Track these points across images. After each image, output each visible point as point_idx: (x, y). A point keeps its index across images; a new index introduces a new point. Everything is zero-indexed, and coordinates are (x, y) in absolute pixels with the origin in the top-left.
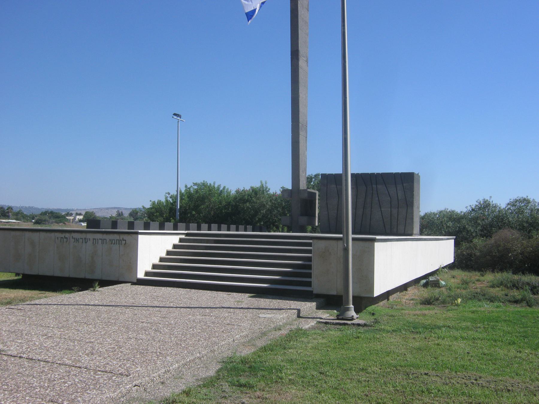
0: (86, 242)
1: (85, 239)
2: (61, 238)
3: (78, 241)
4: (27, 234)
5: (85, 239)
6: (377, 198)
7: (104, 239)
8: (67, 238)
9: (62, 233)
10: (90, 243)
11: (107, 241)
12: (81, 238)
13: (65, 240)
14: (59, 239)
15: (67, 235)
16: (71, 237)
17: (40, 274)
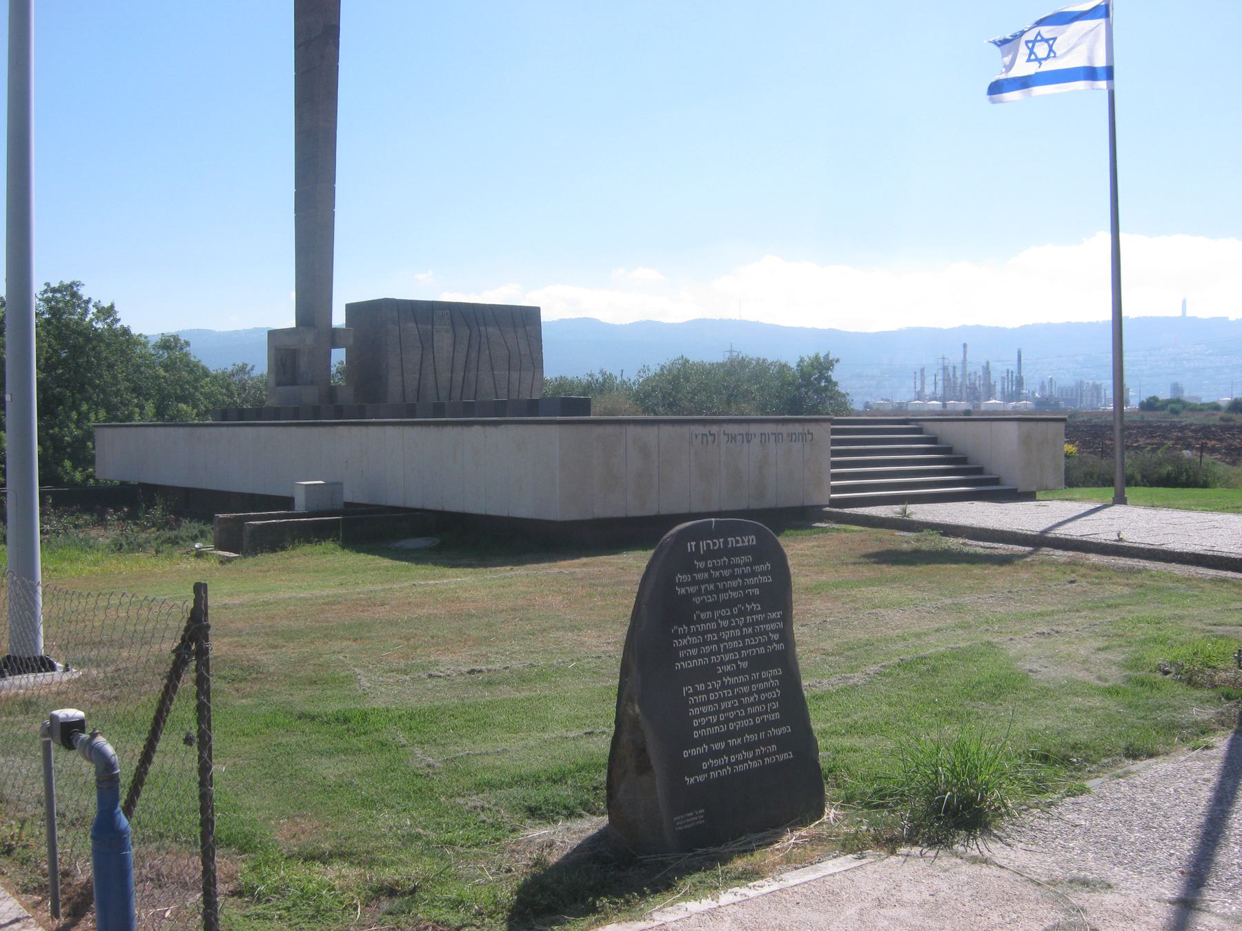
0: (748, 441)
1: (747, 434)
2: (703, 435)
3: (734, 439)
4: (631, 430)
5: (747, 434)
6: (488, 352)
7: (779, 434)
8: (714, 435)
10: (756, 441)
11: (785, 435)
12: (740, 434)
13: (711, 438)
14: (700, 437)
15: (714, 429)
16: (722, 432)
17: (663, 512)
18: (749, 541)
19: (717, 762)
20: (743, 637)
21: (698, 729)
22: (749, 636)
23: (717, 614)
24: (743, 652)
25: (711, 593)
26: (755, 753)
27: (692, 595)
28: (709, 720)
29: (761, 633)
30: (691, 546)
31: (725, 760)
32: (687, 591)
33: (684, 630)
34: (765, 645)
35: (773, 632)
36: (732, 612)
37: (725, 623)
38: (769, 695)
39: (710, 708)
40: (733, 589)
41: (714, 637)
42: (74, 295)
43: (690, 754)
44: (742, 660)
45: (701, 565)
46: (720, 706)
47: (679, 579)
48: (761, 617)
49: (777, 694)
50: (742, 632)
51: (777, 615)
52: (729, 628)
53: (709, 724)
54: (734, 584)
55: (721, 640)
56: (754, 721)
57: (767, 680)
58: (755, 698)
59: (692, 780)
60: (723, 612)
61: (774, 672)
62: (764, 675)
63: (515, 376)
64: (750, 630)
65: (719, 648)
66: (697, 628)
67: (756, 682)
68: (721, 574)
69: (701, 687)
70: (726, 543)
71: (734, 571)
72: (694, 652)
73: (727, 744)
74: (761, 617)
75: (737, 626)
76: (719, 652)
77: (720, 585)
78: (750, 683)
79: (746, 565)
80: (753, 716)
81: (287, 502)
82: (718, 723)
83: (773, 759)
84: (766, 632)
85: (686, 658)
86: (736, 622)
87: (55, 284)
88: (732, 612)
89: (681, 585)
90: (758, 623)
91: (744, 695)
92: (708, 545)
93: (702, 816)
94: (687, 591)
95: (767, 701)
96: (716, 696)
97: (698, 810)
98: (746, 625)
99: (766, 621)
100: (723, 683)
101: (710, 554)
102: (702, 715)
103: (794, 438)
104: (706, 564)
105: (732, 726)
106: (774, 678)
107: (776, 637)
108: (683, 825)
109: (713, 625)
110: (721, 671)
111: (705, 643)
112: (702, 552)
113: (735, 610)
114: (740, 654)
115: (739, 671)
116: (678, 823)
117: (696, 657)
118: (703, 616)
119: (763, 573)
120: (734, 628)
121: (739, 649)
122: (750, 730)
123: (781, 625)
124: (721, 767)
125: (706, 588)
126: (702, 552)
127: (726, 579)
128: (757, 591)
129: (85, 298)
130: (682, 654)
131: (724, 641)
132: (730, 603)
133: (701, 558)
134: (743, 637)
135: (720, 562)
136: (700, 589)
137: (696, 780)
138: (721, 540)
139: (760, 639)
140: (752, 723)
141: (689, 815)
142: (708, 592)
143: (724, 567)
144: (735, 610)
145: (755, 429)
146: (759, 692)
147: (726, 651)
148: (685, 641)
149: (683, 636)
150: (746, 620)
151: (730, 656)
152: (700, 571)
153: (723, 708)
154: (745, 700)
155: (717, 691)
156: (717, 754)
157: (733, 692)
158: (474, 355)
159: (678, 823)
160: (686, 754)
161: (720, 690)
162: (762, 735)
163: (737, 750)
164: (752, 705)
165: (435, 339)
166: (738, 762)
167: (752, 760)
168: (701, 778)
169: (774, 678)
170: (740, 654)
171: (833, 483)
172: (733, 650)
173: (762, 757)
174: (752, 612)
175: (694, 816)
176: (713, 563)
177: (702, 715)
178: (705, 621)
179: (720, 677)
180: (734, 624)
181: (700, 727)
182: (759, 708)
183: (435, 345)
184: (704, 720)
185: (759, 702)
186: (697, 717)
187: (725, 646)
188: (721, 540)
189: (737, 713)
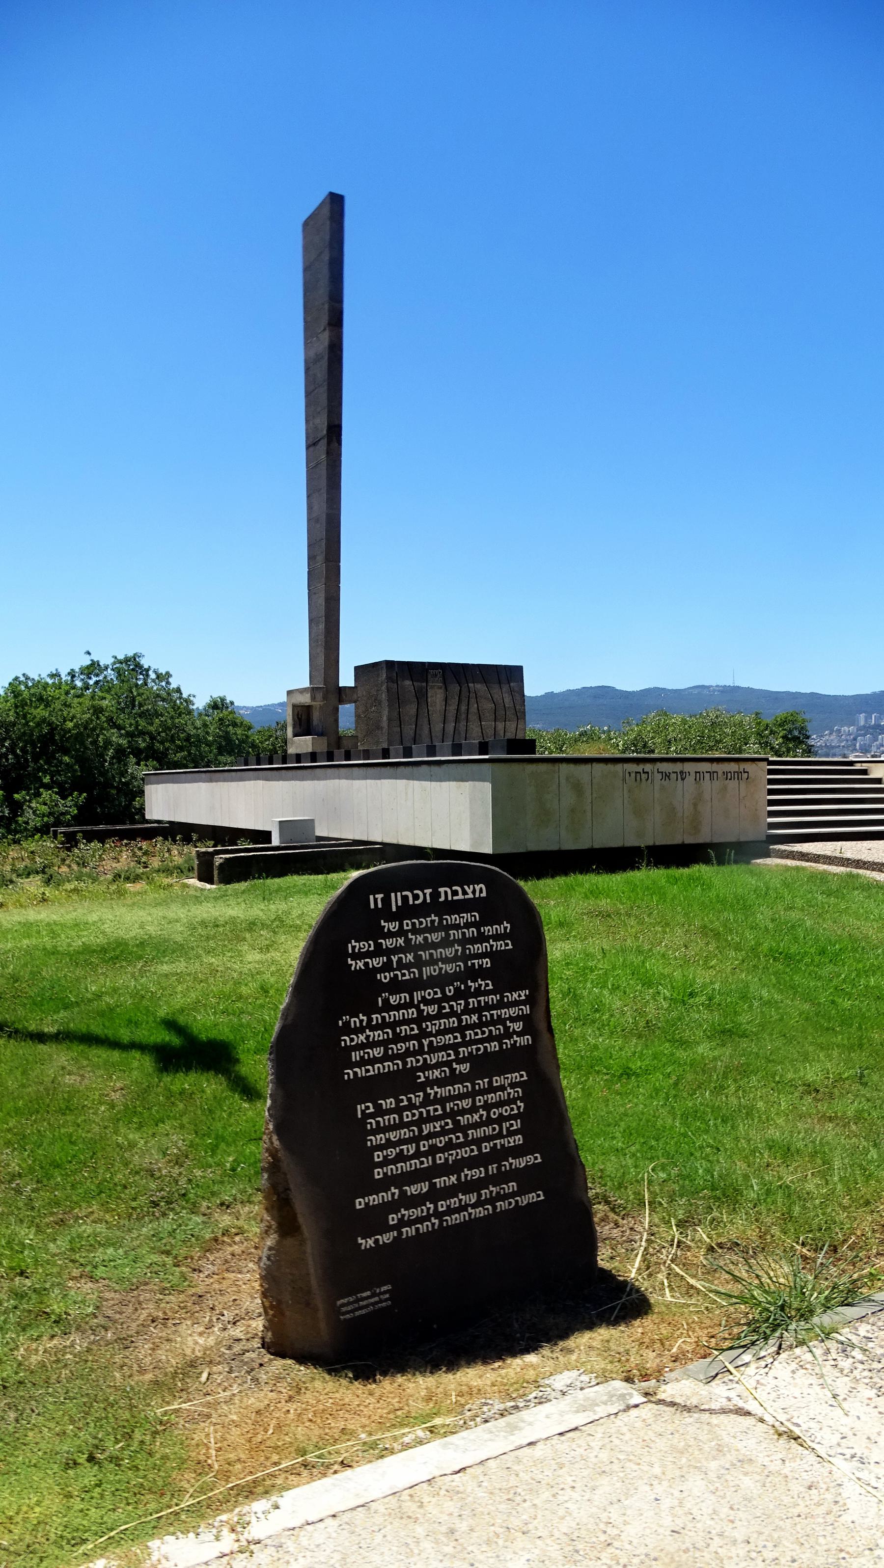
0: (683, 779)
1: (682, 772)
2: (636, 773)
3: (669, 777)
4: (564, 766)
5: (682, 772)
8: (648, 773)
9: (638, 764)
10: (690, 779)
11: (720, 774)
13: (644, 776)
14: (633, 775)
15: (648, 767)
17: (597, 846)
18: (474, 892)
19: (415, 1213)
20: (461, 1029)
21: (381, 1165)
22: (472, 1027)
23: (417, 996)
24: (461, 1050)
25: (408, 966)
26: (479, 1195)
27: (376, 970)
28: (402, 1150)
29: (493, 1022)
30: (376, 900)
31: (429, 1209)
32: (366, 964)
33: (361, 1021)
34: (499, 1038)
35: (512, 1019)
36: (443, 992)
37: (432, 1010)
38: (505, 1111)
39: (405, 1133)
40: (446, 960)
41: (412, 1029)
42: (138, 666)
43: (367, 1204)
44: (459, 1061)
45: (393, 926)
46: (421, 1130)
47: (354, 947)
48: (493, 999)
49: (519, 1108)
50: (460, 1021)
51: (520, 996)
52: (439, 1016)
53: (401, 1157)
54: (449, 952)
55: (424, 1034)
56: (480, 1149)
57: (502, 1088)
58: (481, 1116)
59: (371, 1242)
60: (429, 994)
61: (515, 1077)
62: (497, 1081)
63: (500, 726)
64: (475, 1018)
65: (421, 1045)
66: (383, 1018)
67: (482, 1092)
68: (426, 939)
69: (389, 1103)
70: (435, 895)
71: (447, 935)
72: (378, 1052)
73: (433, 1186)
74: (493, 999)
75: (453, 1013)
76: (421, 1051)
77: (425, 955)
78: (472, 1095)
79: (468, 925)
80: (478, 1142)
81: (265, 836)
82: (418, 1155)
83: (510, 1203)
84: (501, 1021)
85: (362, 1063)
86: (451, 1007)
87: (121, 657)
88: (443, 992)
89: (357, 956)
90: (489, 1007)
91: (463, 1112)
92: (405, 899)
93: (387, 1296)
94: (366, 964)
95: (501, 1119)
96: (414, 1115)
97: (379, 1287)
98: (467, 1011)
99: (500, 1005)
100: (427, 1095)
101: (407, 911)
102: (389, 1144)
103: (729, 777)
104: (401, 925)
105: (440, 1158)
106: (513, 1085)
107: (518, 1026)
108: (352, 1311)
109: (412, 1013)
110: (423, 1079)
111: (397, 1038)
112: (394, 909)
113: (450, 991)
114: (457, 1053)
115: (454, 1078)
116: (344, 1309)
117: (381, 1060)
118: (393, 1000)
119: (497, 937)
120: (447, 1016)
121: (455, 1047)
122: (471, 1163)
123: (526, 1010)
124: (421, 1220)
125: (400, 959)
126: (394, 909)
127: (435, 946)
128: (487, 962)
129: (146, 666)
130: (355, 1056)
131: (430, 1034)
132: (440, 981)
133: (391, 918)
134: (461, 1029)
135: (425, 922)
136: (390, 961)
137: (376, 1241)
138: (428, 891)
139: (490, 1031)
140: (476, 1153)
141: (364, 1295)
142: (401, 965)
143: (432, 929)
144: (450, 991)
145: (689, 767)
146: (487, 1107)
147: (433, 1049)
148: (362, 1038)
149: (360, 1030)
150: (467, 1004)
151: (442, 1056)
152: (391, 935)
153: (425, 1132)
154: (463, 1120)
155: (417, 1108)
156: (416, 1201)
157: (444, 1109)
158: (463, 708)
159: (344, 1309)
160: (360, 1204)
161: (420, 1107)
162: (493, 1168)
163: (450, 1192)
164: (476, 1126)
165: (429, 695)
166: (450, 1211)
167: (474, 1206)
168: (386, 1238)
169: (513, 1085)
170: (457, 1053)
171: (770, 820)
172: (445, 1048)
173: (492, 1201)
174: (478, 992)
175: (374, 1295)
176: (414, 924)
177: (389, 1144)
178: (398, 1007)
179: (422, 1087)
180: (448, 1010)
181: (386, 1162)
182: (488, 1131)
183: (429, 700)
184: (392, 1152)
185: (489, 1122)
186: (380, 1147)
187: (431, 1042)
188: (428, 891)
189: (451, 1139)
